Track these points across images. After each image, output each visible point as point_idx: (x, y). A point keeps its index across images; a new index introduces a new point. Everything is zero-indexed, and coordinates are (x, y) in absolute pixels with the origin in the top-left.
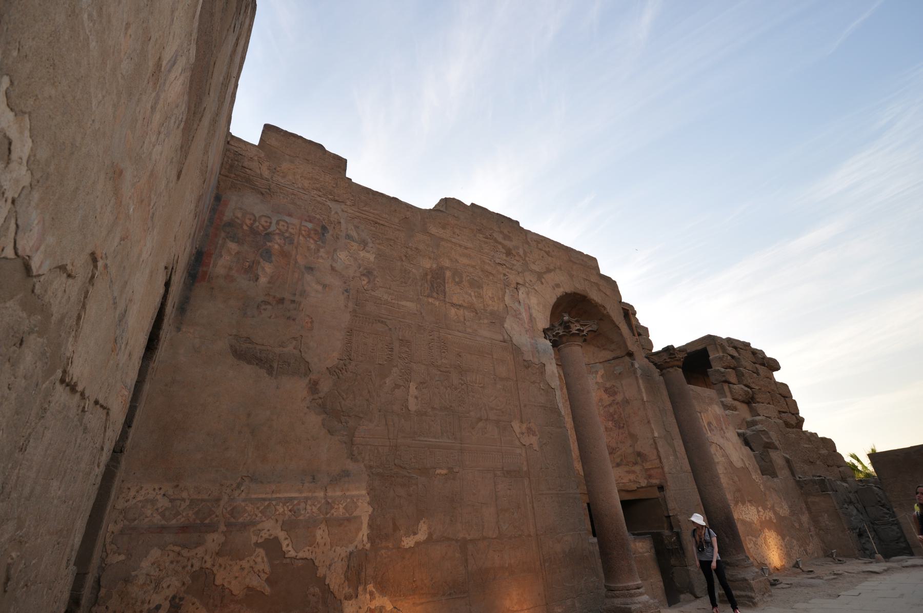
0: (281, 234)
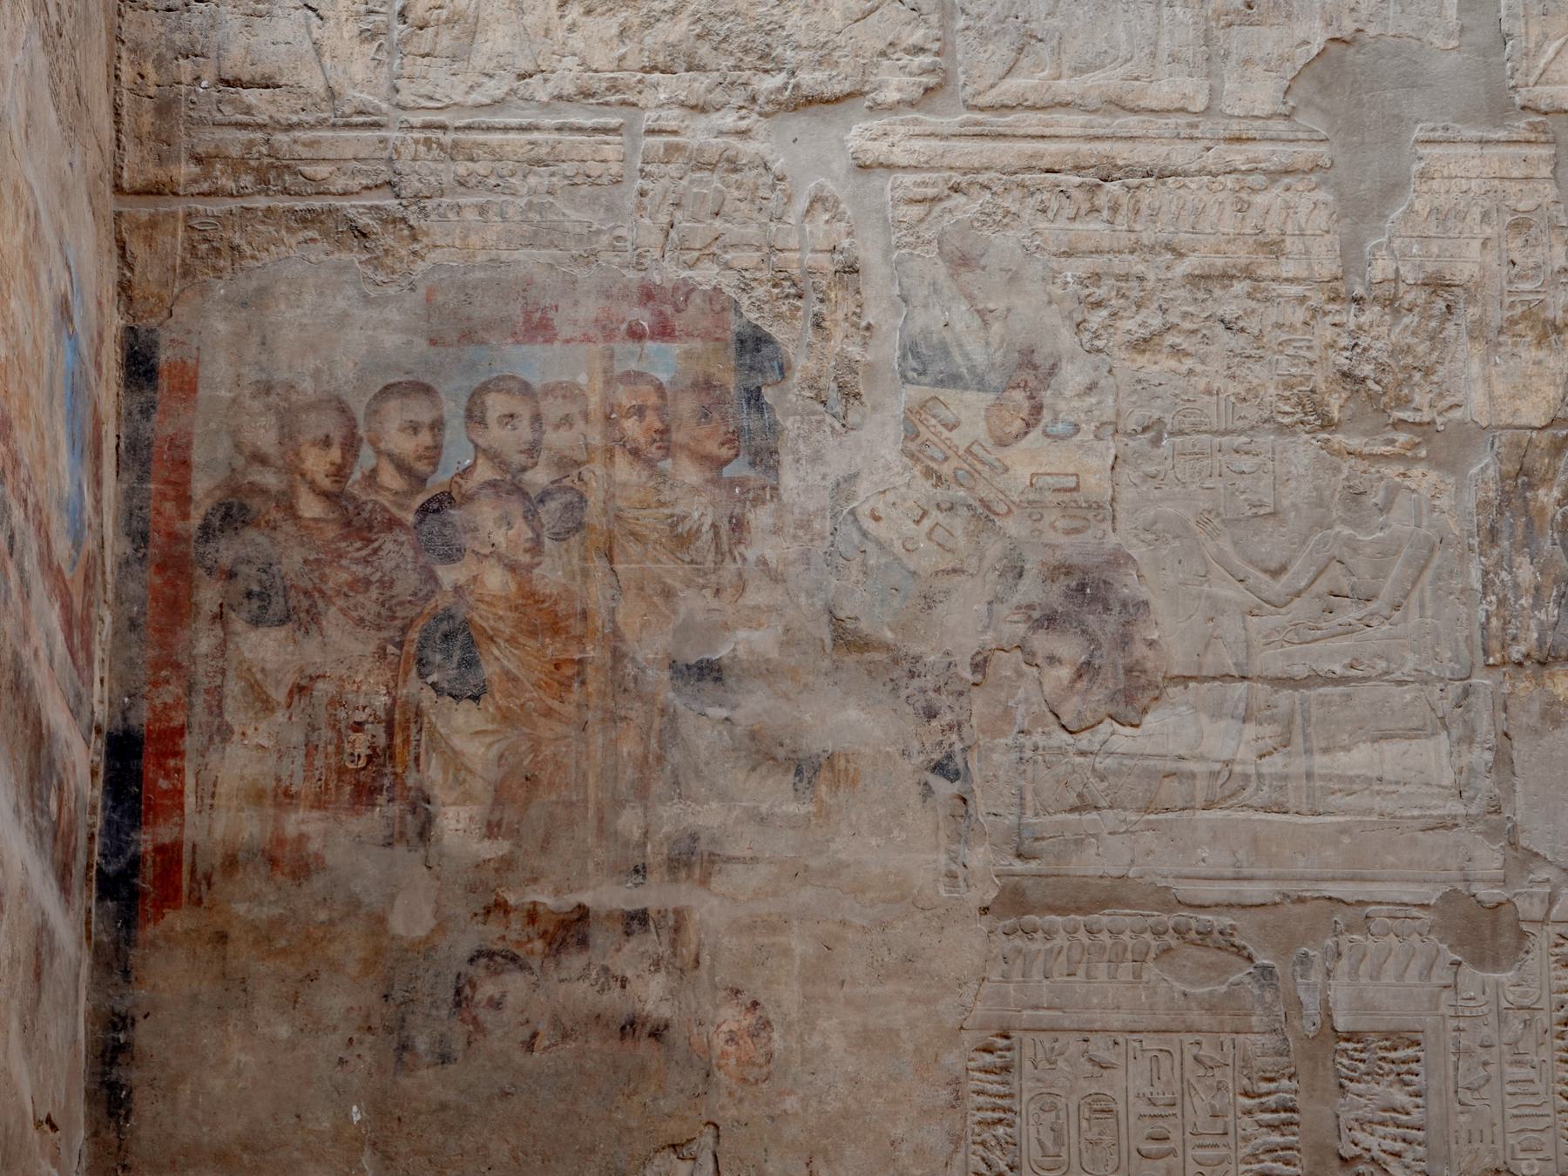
0: (510, 486)
